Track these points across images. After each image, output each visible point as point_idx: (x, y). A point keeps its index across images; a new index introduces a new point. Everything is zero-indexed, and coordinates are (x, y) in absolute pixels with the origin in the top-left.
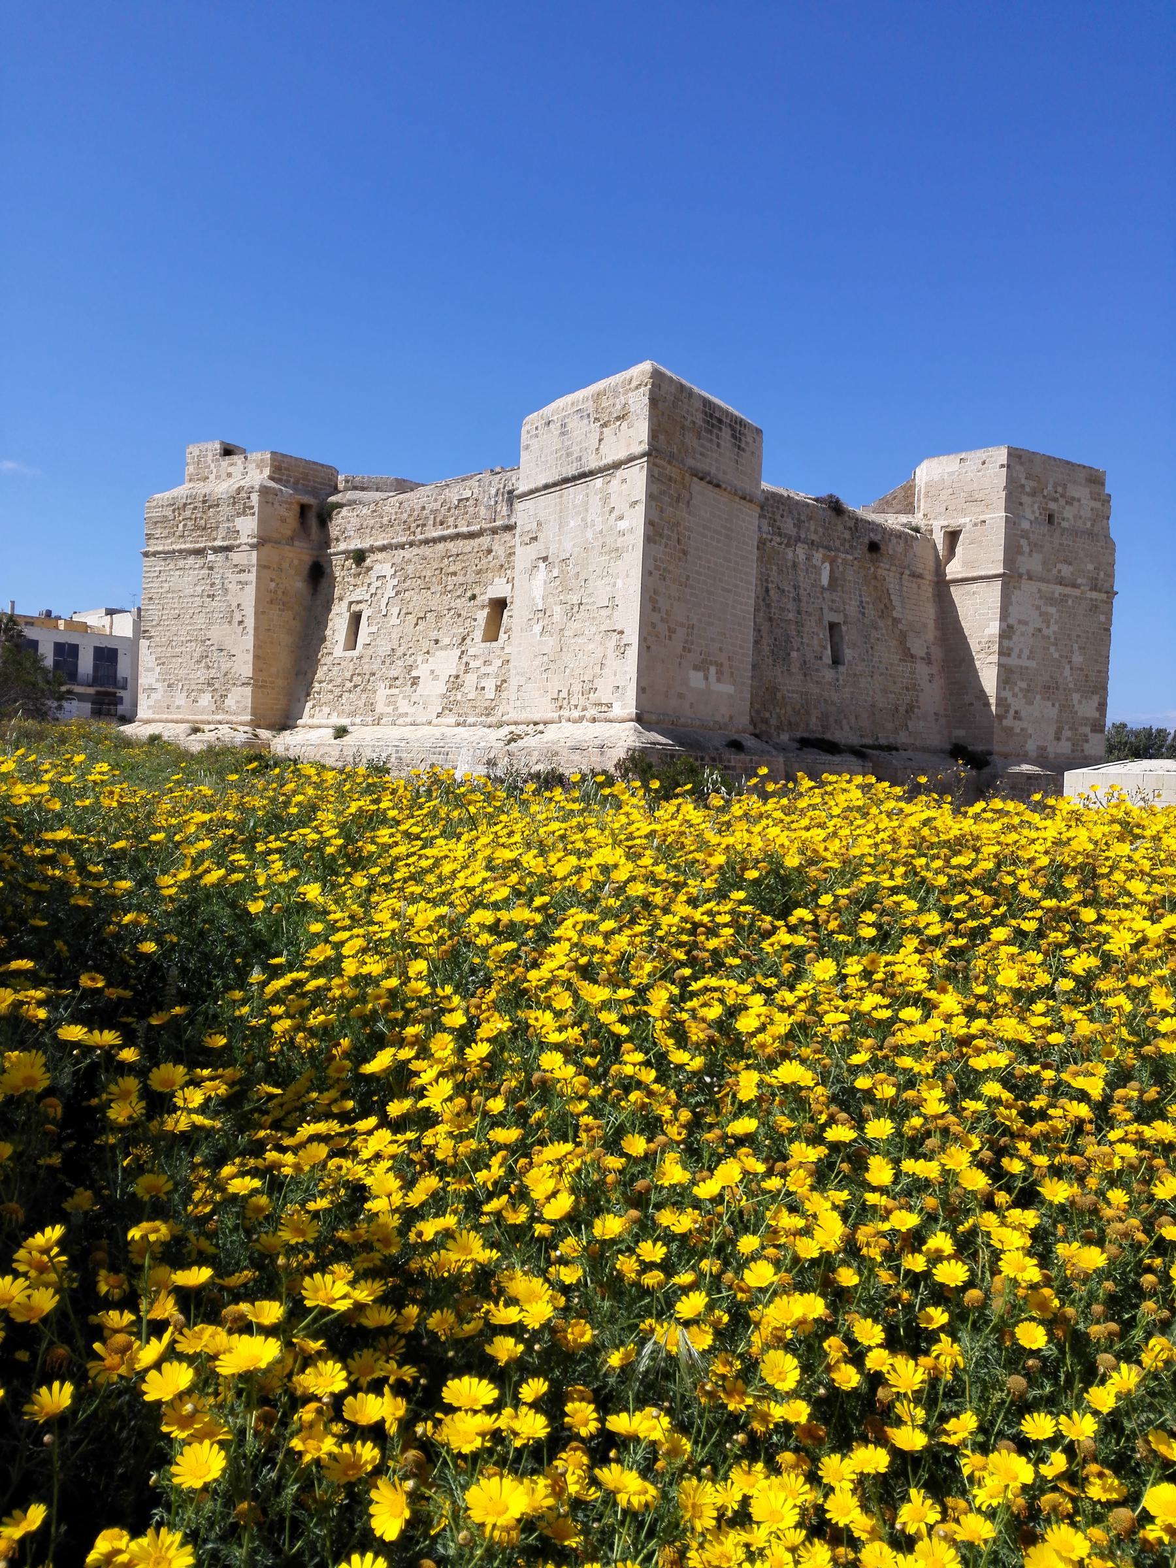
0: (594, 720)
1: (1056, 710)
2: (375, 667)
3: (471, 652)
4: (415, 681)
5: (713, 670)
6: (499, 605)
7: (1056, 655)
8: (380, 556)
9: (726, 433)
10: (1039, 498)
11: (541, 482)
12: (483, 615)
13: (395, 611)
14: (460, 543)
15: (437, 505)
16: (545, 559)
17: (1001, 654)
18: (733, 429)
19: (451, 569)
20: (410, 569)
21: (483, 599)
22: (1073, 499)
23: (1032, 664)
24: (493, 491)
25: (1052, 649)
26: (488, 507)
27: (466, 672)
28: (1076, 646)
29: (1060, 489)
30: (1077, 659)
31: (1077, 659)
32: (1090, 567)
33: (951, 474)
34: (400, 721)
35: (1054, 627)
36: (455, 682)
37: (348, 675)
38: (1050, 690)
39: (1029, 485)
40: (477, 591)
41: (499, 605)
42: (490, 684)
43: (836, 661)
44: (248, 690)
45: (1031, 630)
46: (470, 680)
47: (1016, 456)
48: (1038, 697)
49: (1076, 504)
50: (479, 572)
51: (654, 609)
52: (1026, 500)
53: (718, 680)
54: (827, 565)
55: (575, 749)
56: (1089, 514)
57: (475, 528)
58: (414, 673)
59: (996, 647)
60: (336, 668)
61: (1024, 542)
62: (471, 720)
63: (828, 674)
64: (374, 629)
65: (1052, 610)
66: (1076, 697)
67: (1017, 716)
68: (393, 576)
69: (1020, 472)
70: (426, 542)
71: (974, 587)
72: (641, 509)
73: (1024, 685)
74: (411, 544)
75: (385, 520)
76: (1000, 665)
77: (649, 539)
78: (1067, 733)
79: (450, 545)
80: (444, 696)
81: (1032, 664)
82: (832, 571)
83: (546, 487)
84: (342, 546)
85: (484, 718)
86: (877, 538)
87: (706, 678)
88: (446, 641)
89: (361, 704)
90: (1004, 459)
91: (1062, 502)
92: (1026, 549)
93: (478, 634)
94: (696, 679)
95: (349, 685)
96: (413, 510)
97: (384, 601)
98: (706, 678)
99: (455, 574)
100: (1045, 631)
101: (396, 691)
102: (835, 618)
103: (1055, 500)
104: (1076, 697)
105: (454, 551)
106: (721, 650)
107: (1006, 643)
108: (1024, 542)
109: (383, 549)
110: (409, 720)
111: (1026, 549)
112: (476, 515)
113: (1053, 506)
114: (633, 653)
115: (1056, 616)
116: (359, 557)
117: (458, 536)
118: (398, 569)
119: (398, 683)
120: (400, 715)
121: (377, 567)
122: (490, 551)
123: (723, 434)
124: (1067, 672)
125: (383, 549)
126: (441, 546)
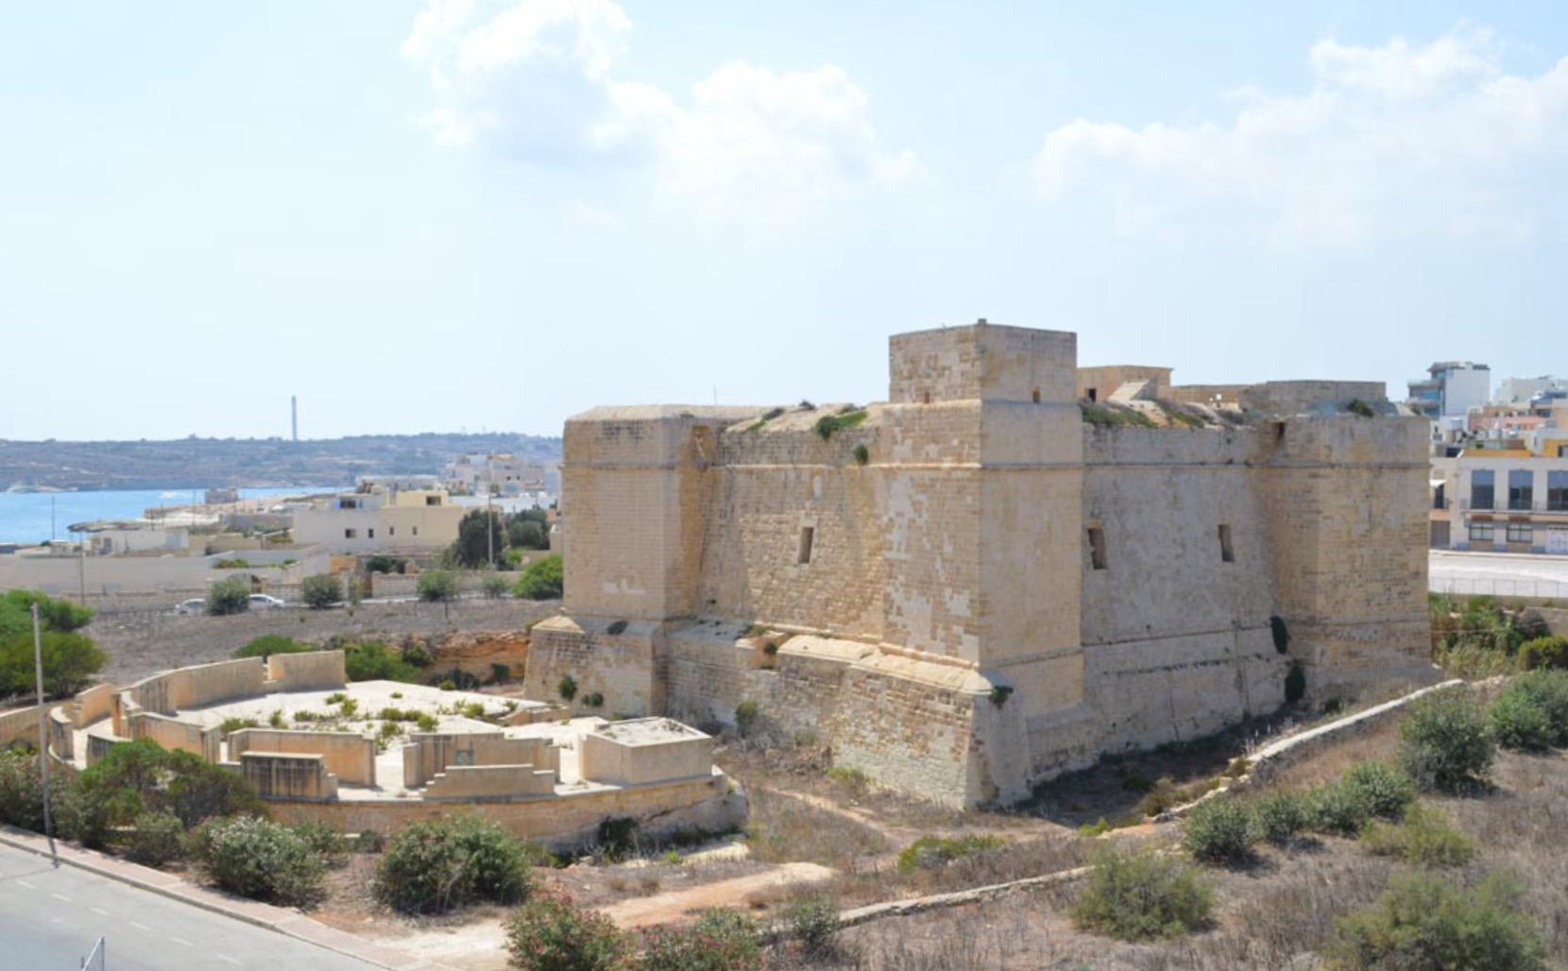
5: (624, 582)
7: (928, 546)
9: (625, 433)
10: (915, 380)
22: (944, 369)
28: (945, 535)
30: (948, 549)
32: (955, 442)
35: (925, 516)
38: (926, 584)
39: (906, 369)
43: (805, 558)
45: (905, 521)
48: (915, 592)
56: (958, 380)
63: (792, 572)
65: (922, 498)
66: (948, 591)
67: (899, 614)
73: (902, 578)
78: (941, 633)
86: (863, 441)
94: (610, 588)
100: (920, 522)
102: (809, 524)
103: (929, 376)
104: (948, 591)
108: (897, 429)
111: (899, 437)
113: (928, 382)
115: (926, 504)
124: (938, 565)
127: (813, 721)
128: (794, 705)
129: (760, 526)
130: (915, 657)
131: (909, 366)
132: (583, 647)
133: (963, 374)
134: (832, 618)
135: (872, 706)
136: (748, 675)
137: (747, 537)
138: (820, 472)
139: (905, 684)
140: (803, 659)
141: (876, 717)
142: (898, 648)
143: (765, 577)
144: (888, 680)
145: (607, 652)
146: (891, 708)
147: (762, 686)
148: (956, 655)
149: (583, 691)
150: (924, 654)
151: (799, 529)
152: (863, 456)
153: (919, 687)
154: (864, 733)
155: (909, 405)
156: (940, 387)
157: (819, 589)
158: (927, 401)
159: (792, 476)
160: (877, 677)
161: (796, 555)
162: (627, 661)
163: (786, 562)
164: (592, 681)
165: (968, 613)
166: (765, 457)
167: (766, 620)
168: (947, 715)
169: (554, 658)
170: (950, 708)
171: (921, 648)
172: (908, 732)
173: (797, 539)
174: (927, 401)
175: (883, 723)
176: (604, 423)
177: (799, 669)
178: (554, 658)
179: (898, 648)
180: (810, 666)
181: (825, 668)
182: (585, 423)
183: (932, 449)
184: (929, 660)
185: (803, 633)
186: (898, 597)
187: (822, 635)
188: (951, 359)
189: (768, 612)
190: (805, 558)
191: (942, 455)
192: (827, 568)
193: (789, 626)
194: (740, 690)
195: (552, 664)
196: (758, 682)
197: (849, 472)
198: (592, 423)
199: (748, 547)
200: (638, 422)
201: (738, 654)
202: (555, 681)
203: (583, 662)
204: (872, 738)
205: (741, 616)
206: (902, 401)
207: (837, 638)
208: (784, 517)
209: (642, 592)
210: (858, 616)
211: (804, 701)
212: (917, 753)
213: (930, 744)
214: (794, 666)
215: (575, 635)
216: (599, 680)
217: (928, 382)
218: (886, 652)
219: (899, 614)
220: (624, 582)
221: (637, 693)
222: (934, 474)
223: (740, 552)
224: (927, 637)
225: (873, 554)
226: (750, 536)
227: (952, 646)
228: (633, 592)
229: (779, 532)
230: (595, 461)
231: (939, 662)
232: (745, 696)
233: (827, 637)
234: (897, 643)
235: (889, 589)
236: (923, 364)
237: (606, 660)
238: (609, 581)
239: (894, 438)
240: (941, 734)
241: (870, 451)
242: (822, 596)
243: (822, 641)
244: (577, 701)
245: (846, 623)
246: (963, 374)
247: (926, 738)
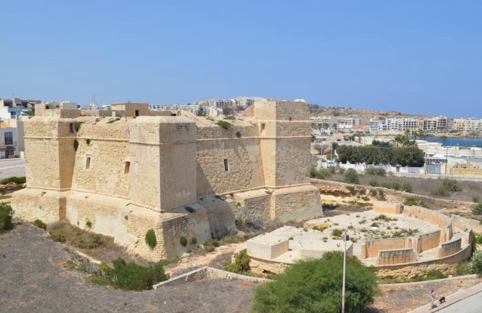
0: (151, 209)
1: (294, 173)
2: (95, 176)
3: (122, 176)
4: (107, 182)
5: (184, 191)
6: (128, 164)
8: (95, 142)
9: (184, 128)
11: (135, 142)
12: (124, 166)
13: (100, 160)
14: (118, 143)
15: (110, 130)
16: (137, 162)
17: (276, 160)
18: (185, 126)
19: (115, 150)
20: (103, 147)
21: (124, 161)
22: (297, 112)
23: (286, 161)
24: (125, 130)
25: (292, 156)
26: (124, 134)
27: (120, 182)
29: (293, 110)
31: (300, 157)
33: (262, 107)
34: (104, 193)
36: (118, 184)
37: (88, 177)
40: (122, 158)
41: (128, 164)
42: (127, 186)
44: (59, 181)
45: (285, 151)
46: (122, 184)
47: (279, 104)
49: (298, 113)
50: (122, 153)
51: (164, 183)
52: (282, 115)
53: (186, 192)
54: (223, 143)
55: (146, 219)
57: (120, 139)
58: (106, 180)
59: (275, 159)
60: (84, 174)
61: (282, 127)
62: (122, 196)
63: (224, 174)
64: (94, 164)
66: (300, 168)
68: (99, 149)
69: (280, 108)
70: (107, 140)
71: (269, 141)
72: (159, 158)
73: (283, 167)
74: (103, 140)
75: (95, 131)
76: (276, 163)
77: (161, 166)
78: (298, 178)
79: (115, 143)
80: (115, 188)
81: (286, 161)
82: (225, 144)
83: (136, 143)
84: (83, 137)
85: (125, 197)
86: (238, 130)
87: (182, 194)
88: (114, 171)
89: (92, 186)
90: (275, 105)
91: (294, 113)
92: (283, 129)
93: (123, 171)
94: (179, 195)
95: (88, 180)
96: (103, 130)
97: (96, 156)
98: (182, 194)
99: (116, 152)
101: (101, 184)
102: (226, 158)
103: (292, 114)
105: (115, 145)
106: (186, 184)
107: (277, 157)
108: (282, 127)
109: (95, 140)
110: (105, 194)
112: (120, 136)
113: (291, 115)
114: (159, 194)
116: (88, 141)
117: (116, 141)
118: (100, 146)
119: (102, 182)
120: (103, 192)
121: (94, 145)
122: (125, 147)
123: (183, 129)
125: (95, 140)
126: (111, 143)
127: (260, 215)
128: (253, 213)
129: (207, 160)
130: (289, 187)
131: (284, 110)
132: (184, 222)
133: (304, 114)
134: (241, 185)
135: (287, 203)
136: (235, 210)
137: (202, 166)
138: (225, 141)
139: (298, 193)
140: (252, 199)
141: (290, 205)
142: (283, 186)
143: (214, 178)
144: (292, 194)
145: (193, 220)
146: (294, 200)
147: (241, 212)
148: (303, 183)
149: (189, 240)
150: (292, 185)
151: (223, 160)
152: (238, 135)
153: (302, 192)
154: (287, 210)
155: (286, 121)
156: (296, 116)
157: (235, 178)
158: (290, 119)
159: (215, 143)
160: (288, 194)
161: (224, 168)
162: (200, 221)
163: (222, 172)
164: (190, 234)
165: (307, 172)
166: (202, 136)
167: (219, 192)
168: (313, 196)
169: (174, 232)
170: (314, 194)
171: (290, 184)
172: (303, 204)
173: (223, 163)
174: (290, 119)
175: (293, 205)
176: (176, 124)
177: (250, 202)
178: (174, 232)
179: (283, 186)
180: (255, 200)
181: (260, 199)
182: (169, 124)
183: (295, 132)
184: (294, 186)
185: (235, 193)
186: (281, 173)
187: (241, 192)
188: (300, 110)
189: (219, 190)
190: (226, 169)
191: (300, 133)
192: (236, 171)
193: (229, 192)
194: (234, 216)
195: (174, 234)
196: (240, 210)
197: (235, 139)
198: (172, 124)
199: (205, 169)
200: (188, 124)
201: (230, 205)
202: (177, 241)
203: (186, 228)
204: (291, 210)
205: (208, 194)
206: (281, 119)
207: (246, 191)
208: (216, 156)
209: (190, 193)
210: (249, 183)
211: (255, 211)
212: (307, 208)
213: (310, 205)
214: (250, 202)
215: (179, 218)
216: (193, 233)
217: (291, 115)
218: (279, 188)
219: (282, 176)
220: (184, 191)
221: (206, 232)
222: (297, 139)
223: (202, 171)
224: (293, 181)
225: (248, 163)
226: (203, 165)
227: (301, 181)
228: (187, 194)
229: (215, 162)
230: (172, 141)
231: (298, 186)
232: (236, 217)
233: (243, 192)
234: (282, 185)
235: (279, 171)
236: (290, 110)
237: (193, 223)
238: (178, 192)
239: (281, 129)
240: (313, 201)
241: (241, 133)
242: (236, 180)
243: (242, 193)
244: (188, 245)
245: (246, 186)
246: (304, 114)
247: (308, 203)
